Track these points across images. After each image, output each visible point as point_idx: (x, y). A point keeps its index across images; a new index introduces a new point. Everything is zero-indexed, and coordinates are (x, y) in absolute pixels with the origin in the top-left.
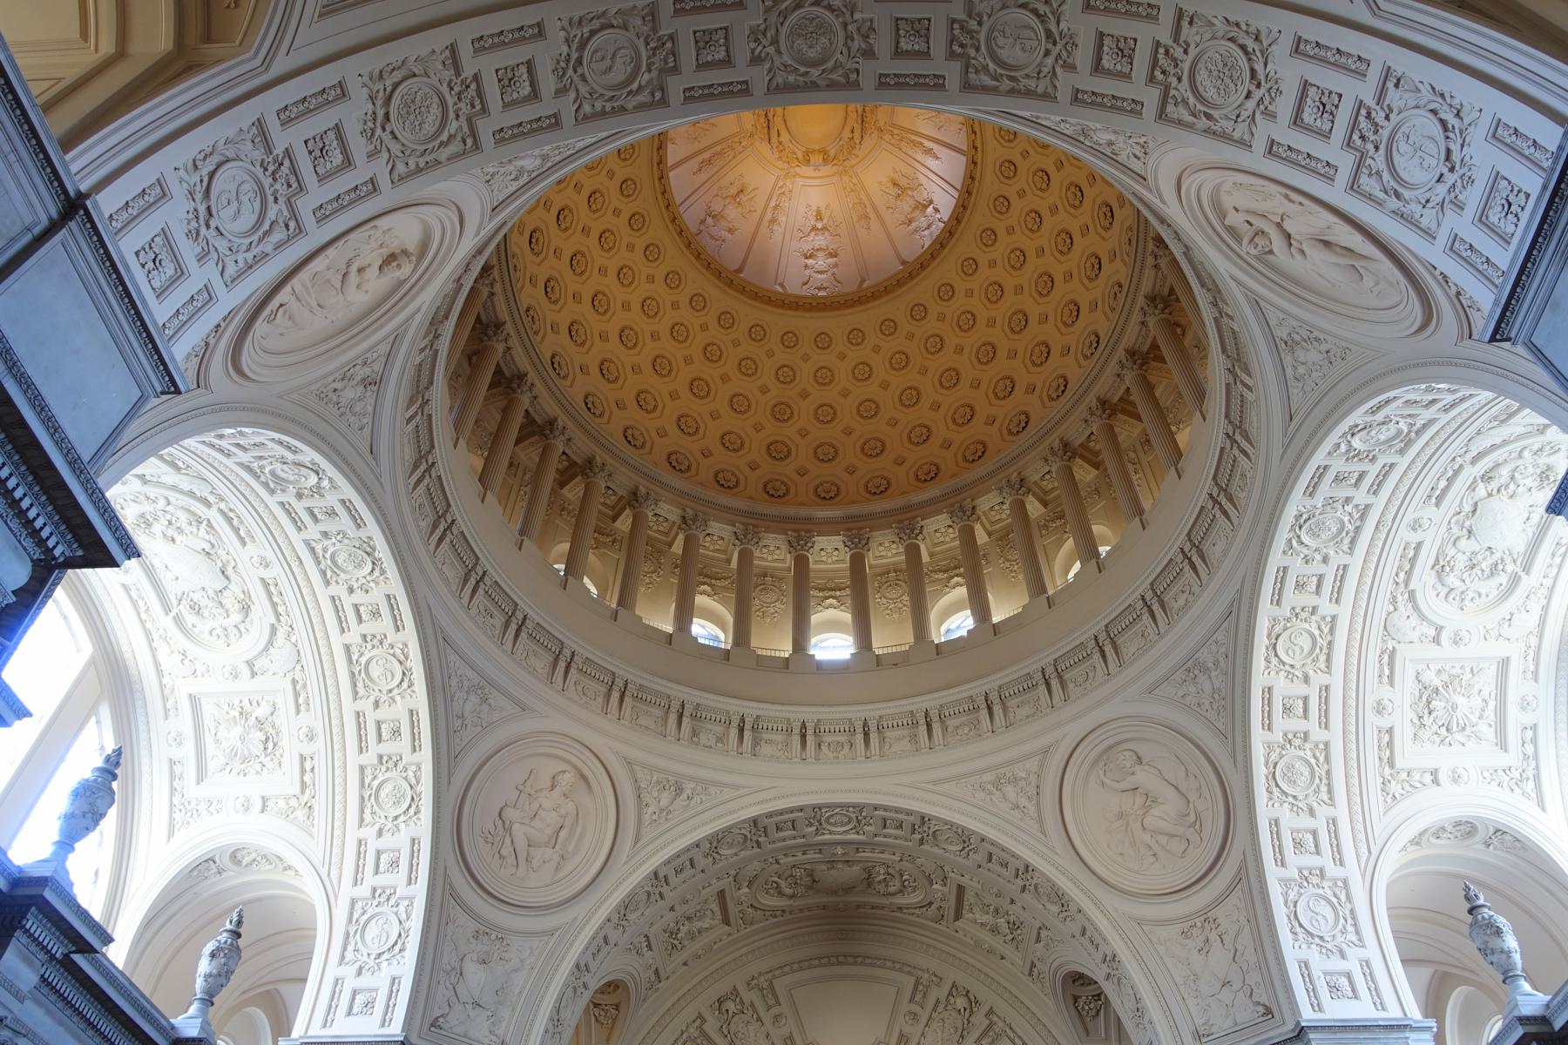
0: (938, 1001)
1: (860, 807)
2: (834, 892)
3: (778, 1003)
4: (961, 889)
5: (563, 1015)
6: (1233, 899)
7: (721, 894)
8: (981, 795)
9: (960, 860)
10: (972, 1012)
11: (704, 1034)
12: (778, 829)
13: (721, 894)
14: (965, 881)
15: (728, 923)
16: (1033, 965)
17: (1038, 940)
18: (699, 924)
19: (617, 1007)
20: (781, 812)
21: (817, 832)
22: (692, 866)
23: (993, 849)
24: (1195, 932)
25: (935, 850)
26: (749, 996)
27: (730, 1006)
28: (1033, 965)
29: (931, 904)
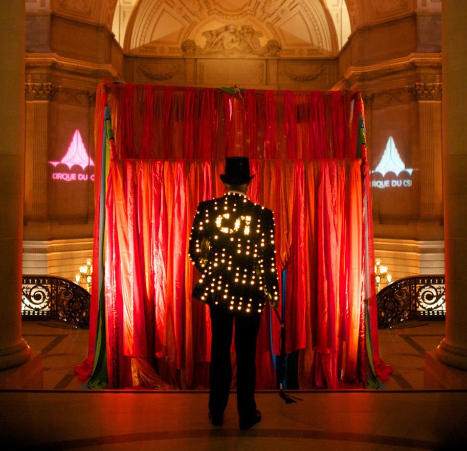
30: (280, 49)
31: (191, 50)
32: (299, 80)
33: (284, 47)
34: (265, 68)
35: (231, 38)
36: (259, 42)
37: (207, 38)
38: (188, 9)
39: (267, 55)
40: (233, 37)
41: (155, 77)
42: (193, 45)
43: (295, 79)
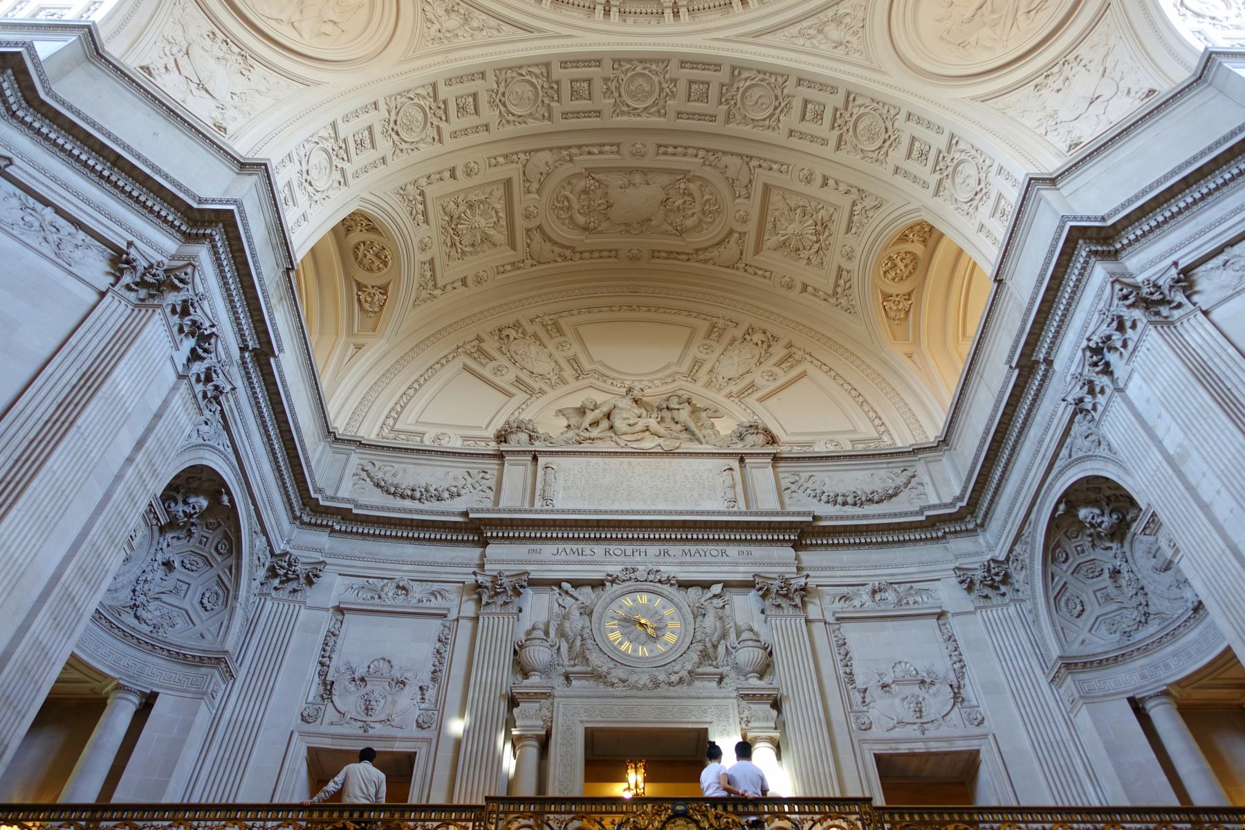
0: (734, 340)
1: (663, 60)
3: (562, 334)
4: (767, 188)
5: (314, 175)
6: (1101, 27)
7: (508, 183)
8: (801, 41)
9: (769, 132)
10: (769, 346)
11: (480, 350)
12: (575, 94)
13: (508, 183)
14: (773, 178)
15: (513, 247)
18: (483, 223)
19: (384, 289)
21: (617, 110)
22: (477, 113)
23: (813, 94)
24: (1051, 79)
25: (741, 127)
26: (530, 329)
27: (512, 333)
28: (840, 269)
29: (731, 231)
30: (773, 440)
31: (524, 437)
38: (523, 368)
41: (409, 493)
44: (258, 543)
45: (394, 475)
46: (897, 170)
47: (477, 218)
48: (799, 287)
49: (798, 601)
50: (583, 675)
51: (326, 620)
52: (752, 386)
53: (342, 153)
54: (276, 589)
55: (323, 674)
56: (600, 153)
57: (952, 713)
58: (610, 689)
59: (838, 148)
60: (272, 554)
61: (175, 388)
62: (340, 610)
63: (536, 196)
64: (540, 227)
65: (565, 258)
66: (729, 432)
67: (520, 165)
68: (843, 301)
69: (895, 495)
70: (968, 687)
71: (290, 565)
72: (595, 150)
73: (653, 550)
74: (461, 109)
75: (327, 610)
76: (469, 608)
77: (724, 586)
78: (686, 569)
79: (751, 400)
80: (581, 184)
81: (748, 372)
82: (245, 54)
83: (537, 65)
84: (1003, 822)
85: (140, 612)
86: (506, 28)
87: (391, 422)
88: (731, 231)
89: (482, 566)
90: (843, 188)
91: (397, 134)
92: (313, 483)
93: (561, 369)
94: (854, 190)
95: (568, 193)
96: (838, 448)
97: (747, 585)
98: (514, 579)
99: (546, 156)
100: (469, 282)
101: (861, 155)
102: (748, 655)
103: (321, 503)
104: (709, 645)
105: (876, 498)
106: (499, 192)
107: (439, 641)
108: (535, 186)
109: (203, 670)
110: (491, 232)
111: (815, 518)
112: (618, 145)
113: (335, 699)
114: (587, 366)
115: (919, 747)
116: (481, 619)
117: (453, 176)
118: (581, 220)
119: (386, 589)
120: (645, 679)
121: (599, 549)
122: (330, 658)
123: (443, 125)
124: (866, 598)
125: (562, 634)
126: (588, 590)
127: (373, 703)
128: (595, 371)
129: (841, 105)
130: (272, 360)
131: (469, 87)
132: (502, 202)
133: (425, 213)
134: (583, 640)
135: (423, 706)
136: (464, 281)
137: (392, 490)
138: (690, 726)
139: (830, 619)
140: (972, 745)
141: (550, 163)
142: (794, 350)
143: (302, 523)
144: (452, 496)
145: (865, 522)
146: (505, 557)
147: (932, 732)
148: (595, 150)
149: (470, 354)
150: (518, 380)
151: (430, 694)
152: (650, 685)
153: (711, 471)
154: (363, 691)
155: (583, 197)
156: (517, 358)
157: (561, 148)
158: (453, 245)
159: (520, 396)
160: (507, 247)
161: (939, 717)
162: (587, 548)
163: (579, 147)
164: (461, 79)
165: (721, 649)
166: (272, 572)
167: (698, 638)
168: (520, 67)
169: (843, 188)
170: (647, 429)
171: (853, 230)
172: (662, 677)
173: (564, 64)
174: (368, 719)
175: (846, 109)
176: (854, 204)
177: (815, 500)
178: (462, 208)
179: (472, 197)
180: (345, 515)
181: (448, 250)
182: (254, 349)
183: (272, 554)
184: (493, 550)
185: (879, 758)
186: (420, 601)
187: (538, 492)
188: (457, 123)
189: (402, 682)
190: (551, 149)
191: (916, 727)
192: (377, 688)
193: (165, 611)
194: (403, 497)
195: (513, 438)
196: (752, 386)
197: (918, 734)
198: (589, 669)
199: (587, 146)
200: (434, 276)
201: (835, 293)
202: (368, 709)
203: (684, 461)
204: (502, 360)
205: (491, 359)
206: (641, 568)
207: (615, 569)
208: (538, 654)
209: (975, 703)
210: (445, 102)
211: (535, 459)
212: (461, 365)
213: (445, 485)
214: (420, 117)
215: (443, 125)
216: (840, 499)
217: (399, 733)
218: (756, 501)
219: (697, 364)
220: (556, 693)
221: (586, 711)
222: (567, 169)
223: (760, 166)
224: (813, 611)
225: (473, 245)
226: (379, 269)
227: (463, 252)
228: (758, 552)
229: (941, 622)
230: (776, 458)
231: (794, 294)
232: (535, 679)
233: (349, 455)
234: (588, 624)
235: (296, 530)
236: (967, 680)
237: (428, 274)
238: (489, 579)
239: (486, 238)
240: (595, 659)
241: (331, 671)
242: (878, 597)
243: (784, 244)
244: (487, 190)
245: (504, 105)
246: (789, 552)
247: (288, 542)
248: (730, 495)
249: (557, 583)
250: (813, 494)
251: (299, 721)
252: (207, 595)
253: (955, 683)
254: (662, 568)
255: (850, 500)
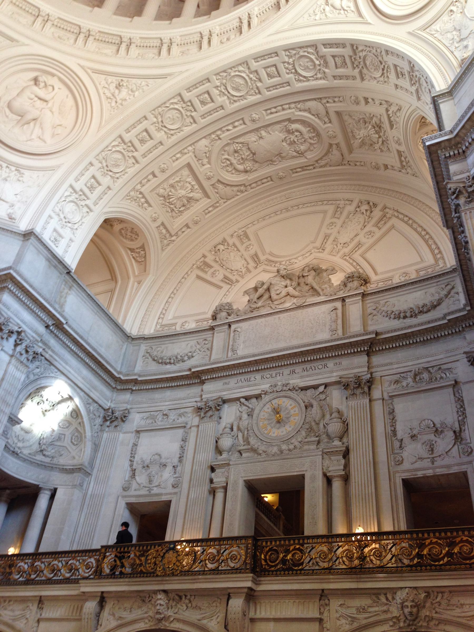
2: (271, 162)
3: (249, 240)
5: (70, 216)
10: (371, 212)
15: (208, 197)
16: (400, 153)
17: (392, 126)
19: (143, 247)
20: (195, 86)
26: (231, 241)
27: (221, 247)
30: (366, 281)
32: (405, 317)
33: (373, 277)
34: (339, 312)
35: (284, 283)
36: (330, 280)
37: (249, 296)
39: (342, 292)
40: (288, 282)
41: (168, 361)
42: (227, 308)
43: (398, 317)
44: (91, 408)
45: (162, 352)
46: (396, 86)
47: (179, 191)
48: (382, 168)
49: (366, 389)
50: (247, 450)
51: (130, 438)
52: (359, 245)
53: (83, 197)
54: (108, 427)
55: (131, 466)
56: (235, 127)
57: (453, 449)
58: (259, 457)
59: (363, 79)
60: (105, 410)
61: (9, 363)
62: (138, 432)
63: (209, 166)
64: (219, 181)
65: (242, 192)
66: (339, 283)
67: (191, 154)
68: (409, 170)
69: (439, 304)
70: (467, 432)
71: (113, 414)
72: (230, 127)
73: (286, 371)
74: (142, 141)
75: (132, 432)
76: (196, 421)
77: (325, 388)
78: (304, 379)
79: (357, 256)
80: (231, 149)
81: (356, 236)
82: (19, 168)
83: (173, 98)
84: (317, 543)
85: (44, 453)
86: (150, 81)
87: (160, 321)
88: (331, 145)
89: (201, 396)
90: (377, 102)
91: (111, 171)
92: (115, 370)
93: (248, 264)
94: (383, 102)
95: (226, 156)
96: (407, 278)
97: (338, 383)
98: (215, 401)
99: (204, 142)
100: (190, 225)
101: (376, 81)
102: (335, 427)
103: (123, 378)
104: (313, 424)
105: (425, 310)
106: (186, 172)
107: (183, 440)
108: (205, 161)
109: (75, 474)
110: (191, 195)
111: (377, 334)
112: (242, 119)
113: (137, 477)
114: (262, 258)
115: (430, 473)
116: (200, 427)
117: (155, 176)
118: (241, 167)
119: (158, 417)
120: (275, 449)
121: (258, 376)
122: (134, 457)
123: (135, 154)
124: (410, 380)
125: (239, 429)
126: (254, 400)
127: (152, 478)
128: (267, 260)
129: (351, 54)
130: (65, 326)
131: (140, 128)
132: (191, 176)
133: (147, 202)
134: (248, 431)
135: (175, 476)
136: (187, 226)
137: (160, 361)
138: (295, 474)
139: (386, 397)
140: (463, 468)
141: (207, 144)
142: (387, 210)
143: (118, 390)
144: (189, 358)
145: (410, 331)
146: (212, 390)
147: (439, 462)
148: (230, 127)
149: (198, 268)
150: (225, 277)
151: (179, 469)
152: (278, 452)
153: (324, 313)
154: (149, 471)
155: (236, 155)
156: (224, 263)
157: (210, 135)
158: (172, 210)
159: (226, 287)
160: (205, 199)
161: (444, 453)
162: (252, 376)
163: (220, 129)
164: (133, 126)
165: (321, 426)
166: (105, 420)
167: (307, 421)
168: (165, 103)
169: (377, 102)
170: (288, 294)
171: (395, 126)
172: (284, 447)
173: (189, 90)
174: (151, 486)
175: (356, 54)
176: (387, 110)
177: (387, 318)
178: (168, 190)
179: (171, 181)
180: (135, 382)
181: (170, 214)
182: (53, 324)
183: (105, 410)
184: (208, 387)
185: (403, 480)
186: (174, 420)
187: (230, 347)
188: (143, 149)
189: (165, 465)
190: (205, 137)
191: (429, 460)
192: (154, 469)
193: (56, 449)
194: (166, 364)
195: (218, 316)
196: (359, 245)
197: (430, 465)
198: (249, 447)
199: (224, 127)
200: (167, 231)
201: (403, 167)
202: (150, 481)
203: (310, 310)
204: (216, 266)
205: (211, 267)
206: (279, 384)
207: (266, 387)
208: (226, 442)
209: (469, 441)
210: (130, 142)
211: (230, 326)
212: (195, 275)
213: (186, 352)
214: (119, 156)
215: (135, 154)
216: (402, 315)
217: (163, 491)
218: (350, 327)
219: (327, 237)
220: (231, 463)
221: (244, 471)
222: (219, 144)
223: (328, 102)
224: (376, 394)
225: (184, 206)
226: (136, 239)
227: (180, 211)
228: (345, 362)
229: (455, 390)
230: (364, 295)
231: (382, 172)
232: (225, 455)
233: (140, 345)
234: (250, 421)
235: (115, 395)
236: (466, 426)
237: (164, 231)
238: (203, 403)
239: (190, 199)
240: (253, 441)
241: (135, 463)
242: (418, 378)
243: (363, 144)
244: (179, 174)
245: (165, 127)
246: (364, 358)
247: (111, 402)
248: (334, 327)
249: (238, 399)
250: (386, 315)
251: (122, 491)
252: (74, 438)
253: (458, 429)
254: (291, 382)
255: (408, 314)
